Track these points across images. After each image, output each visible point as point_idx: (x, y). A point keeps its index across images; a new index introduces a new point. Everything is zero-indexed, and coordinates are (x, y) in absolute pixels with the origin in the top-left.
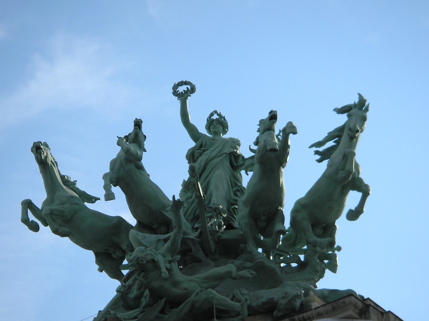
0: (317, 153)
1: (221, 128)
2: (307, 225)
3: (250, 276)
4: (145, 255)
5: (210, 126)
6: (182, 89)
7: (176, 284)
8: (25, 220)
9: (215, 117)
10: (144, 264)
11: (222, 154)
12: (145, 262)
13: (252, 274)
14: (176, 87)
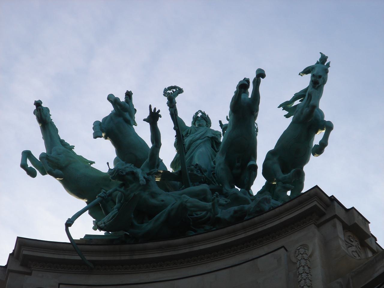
2: (277, 167)
3: (225, 203)
4: (125, 168)
5: (195, 121)
8: (24, 166)
10: (124, 176)
11: (205, 138)
12: (125, 174)
14: (165, 90)
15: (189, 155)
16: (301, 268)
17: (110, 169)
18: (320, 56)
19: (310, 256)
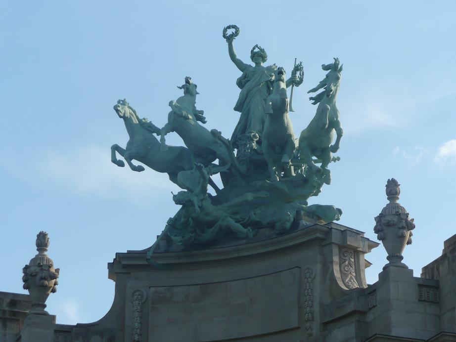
0: (311, 99)
1: (261, 59)
3: (265, 196)
6: (230, 32)
7: (207, 214)
8: (114, 160)
9: (257, 50)
13: (266, 195)
14: (225, 30)
15: (247, 106)
16: (306, 291)
17: (174, 195)
18: (333, 62)
19: (314, 279)
